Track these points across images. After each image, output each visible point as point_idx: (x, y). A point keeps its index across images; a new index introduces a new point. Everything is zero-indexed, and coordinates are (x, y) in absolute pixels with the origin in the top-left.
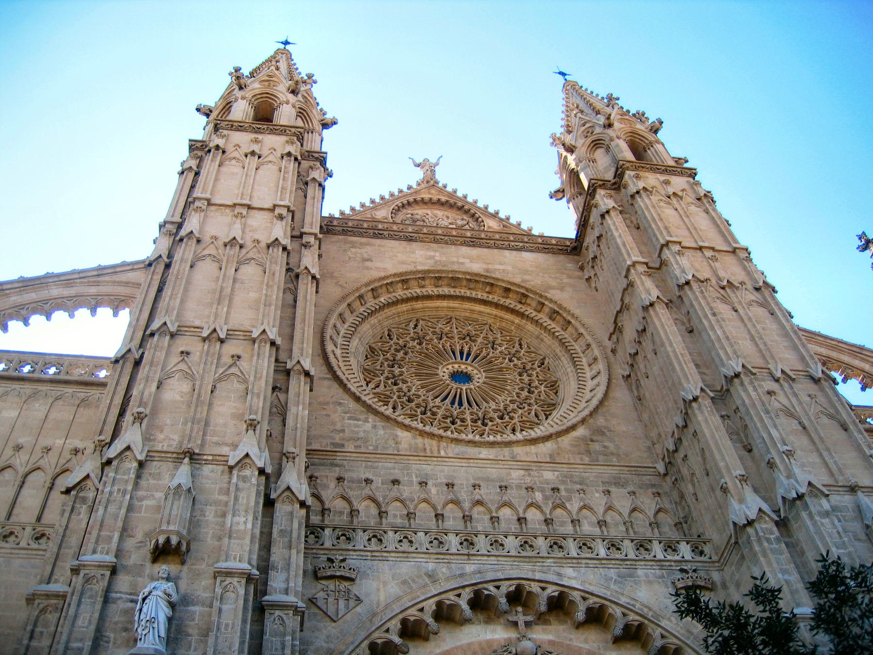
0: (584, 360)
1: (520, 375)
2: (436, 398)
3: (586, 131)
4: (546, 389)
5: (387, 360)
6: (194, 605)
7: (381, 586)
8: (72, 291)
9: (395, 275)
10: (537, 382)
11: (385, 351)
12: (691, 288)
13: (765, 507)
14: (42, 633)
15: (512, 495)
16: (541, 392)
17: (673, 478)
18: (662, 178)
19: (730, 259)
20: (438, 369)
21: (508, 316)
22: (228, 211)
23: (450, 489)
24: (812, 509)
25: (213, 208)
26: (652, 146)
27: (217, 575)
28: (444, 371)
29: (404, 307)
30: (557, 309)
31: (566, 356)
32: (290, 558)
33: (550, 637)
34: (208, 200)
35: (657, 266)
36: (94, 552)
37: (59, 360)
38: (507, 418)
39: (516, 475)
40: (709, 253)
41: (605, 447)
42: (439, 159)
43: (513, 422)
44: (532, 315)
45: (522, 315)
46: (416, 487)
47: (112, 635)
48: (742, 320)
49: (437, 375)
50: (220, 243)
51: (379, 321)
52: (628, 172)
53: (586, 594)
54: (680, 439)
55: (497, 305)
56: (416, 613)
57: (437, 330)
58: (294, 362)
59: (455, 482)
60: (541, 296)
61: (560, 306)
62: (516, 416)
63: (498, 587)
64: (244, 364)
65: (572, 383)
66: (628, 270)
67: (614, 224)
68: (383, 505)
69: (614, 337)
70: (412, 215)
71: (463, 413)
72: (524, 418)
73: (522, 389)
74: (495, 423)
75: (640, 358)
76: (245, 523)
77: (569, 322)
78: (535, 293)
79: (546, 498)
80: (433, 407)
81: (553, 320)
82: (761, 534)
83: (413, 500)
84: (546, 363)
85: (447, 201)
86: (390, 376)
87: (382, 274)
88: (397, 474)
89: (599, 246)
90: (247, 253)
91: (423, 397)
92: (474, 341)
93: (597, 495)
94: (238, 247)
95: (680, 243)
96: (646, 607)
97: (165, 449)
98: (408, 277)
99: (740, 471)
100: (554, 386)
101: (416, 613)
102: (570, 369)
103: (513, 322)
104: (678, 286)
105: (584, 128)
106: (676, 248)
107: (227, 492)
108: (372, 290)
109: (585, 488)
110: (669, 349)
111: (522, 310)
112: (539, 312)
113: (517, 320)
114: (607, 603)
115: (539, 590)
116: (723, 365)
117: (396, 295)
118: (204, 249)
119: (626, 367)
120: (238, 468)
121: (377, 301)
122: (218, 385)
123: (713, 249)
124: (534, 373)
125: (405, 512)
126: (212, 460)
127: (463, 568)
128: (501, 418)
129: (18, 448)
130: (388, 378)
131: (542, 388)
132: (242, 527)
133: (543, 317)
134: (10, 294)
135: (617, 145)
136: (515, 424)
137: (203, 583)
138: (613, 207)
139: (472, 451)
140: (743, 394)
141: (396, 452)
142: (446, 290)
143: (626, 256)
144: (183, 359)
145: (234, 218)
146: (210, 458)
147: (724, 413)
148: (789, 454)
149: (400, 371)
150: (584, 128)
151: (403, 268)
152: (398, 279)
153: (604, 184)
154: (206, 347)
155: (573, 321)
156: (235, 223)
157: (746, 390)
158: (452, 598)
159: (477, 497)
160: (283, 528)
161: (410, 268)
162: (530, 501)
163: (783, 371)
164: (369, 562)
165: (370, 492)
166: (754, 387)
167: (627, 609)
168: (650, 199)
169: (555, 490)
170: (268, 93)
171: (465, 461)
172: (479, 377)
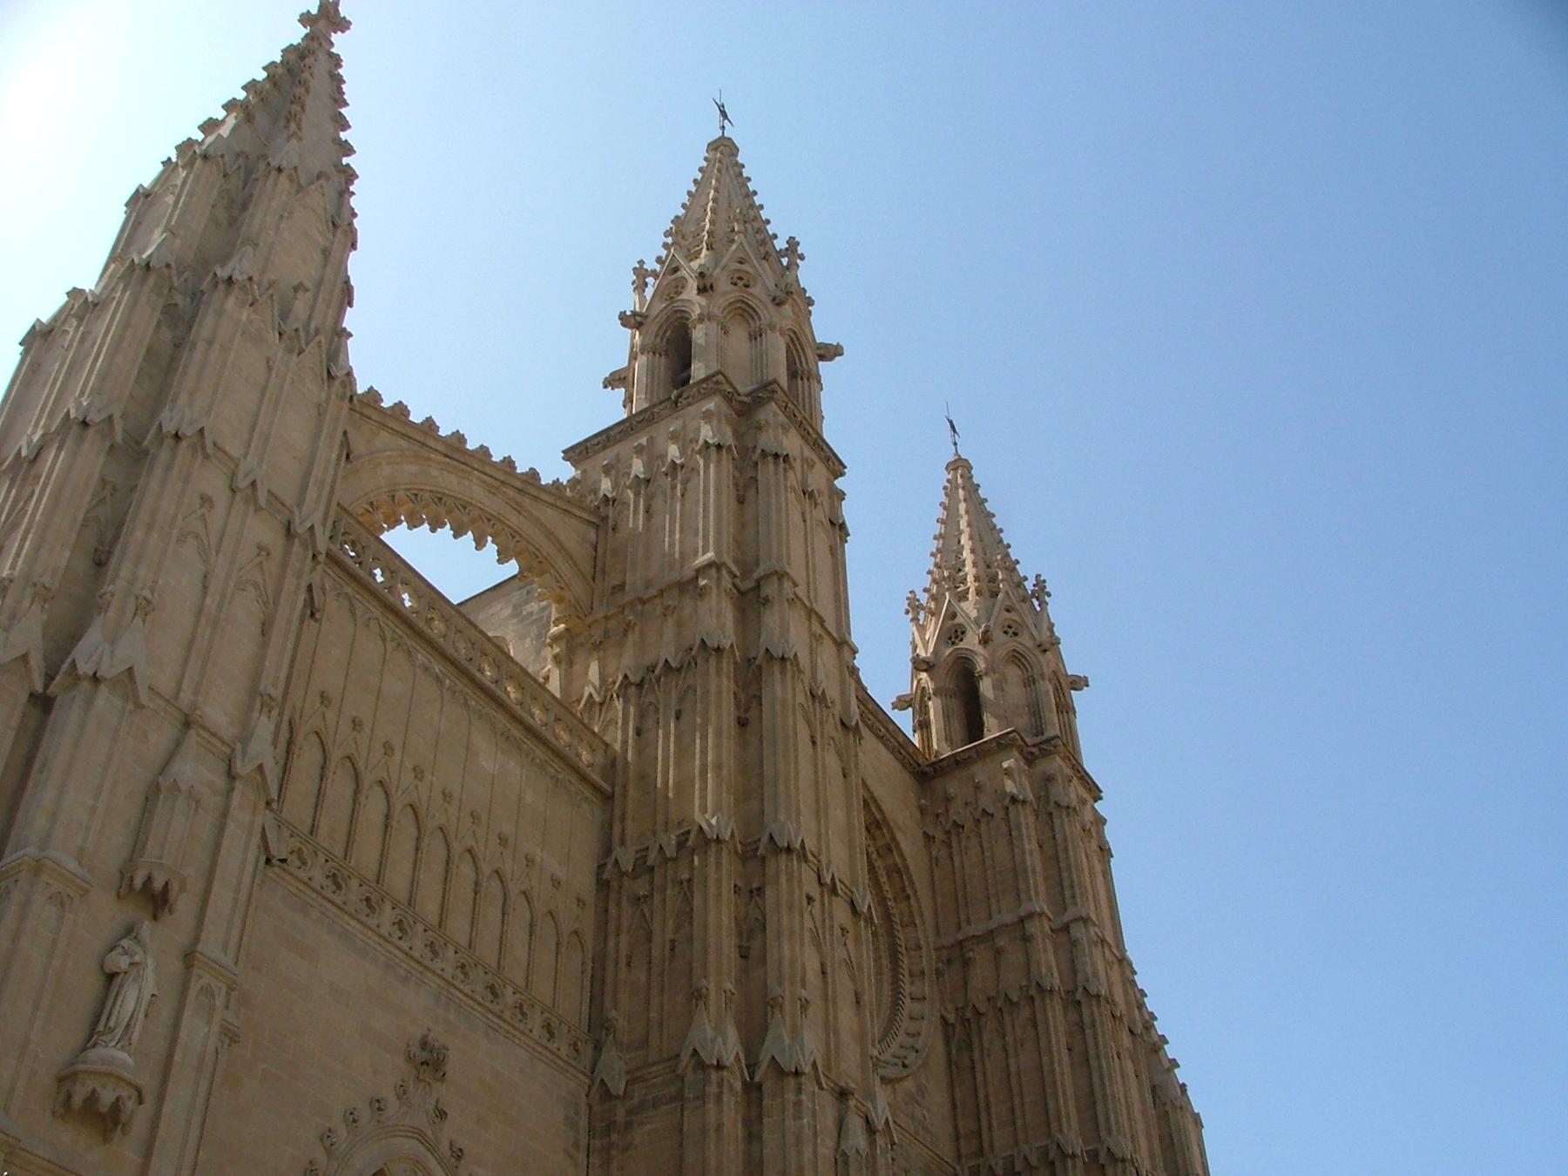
12: (1099, 1002)
30: (900, 866)
41: (924, 1117)
61: (907, 867)
69: (945, 953)
77: (908, 897)
119: (949, 1006)
123: (1110, 946)
135: (1047, 692)
155: (912, 901)
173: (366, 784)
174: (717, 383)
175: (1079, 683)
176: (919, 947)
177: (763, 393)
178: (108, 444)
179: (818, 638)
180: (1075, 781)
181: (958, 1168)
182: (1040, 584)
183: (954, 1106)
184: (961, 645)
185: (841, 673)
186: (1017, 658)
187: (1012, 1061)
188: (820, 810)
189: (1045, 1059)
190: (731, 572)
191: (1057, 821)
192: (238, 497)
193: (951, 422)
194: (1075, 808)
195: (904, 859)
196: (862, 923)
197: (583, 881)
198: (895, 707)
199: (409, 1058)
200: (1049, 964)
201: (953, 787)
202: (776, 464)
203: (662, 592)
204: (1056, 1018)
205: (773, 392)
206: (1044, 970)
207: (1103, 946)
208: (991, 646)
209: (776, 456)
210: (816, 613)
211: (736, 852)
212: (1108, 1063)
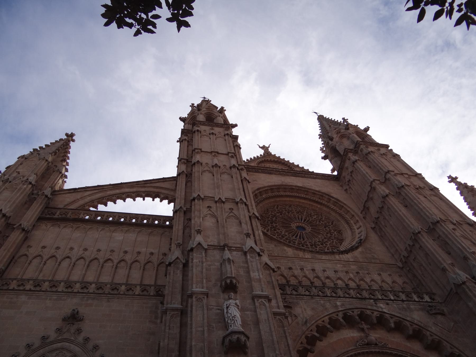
0: (352, 221)
1: (325, 227)
2: (293, 236)
3: (337, 132)
4: (337, 234)
5: (269, 220)
6: (247, 311)
7: (304, 310)
8: (134, 190)
9: (268, 186)
10: (333, 231)
11: (268, 217)
12: (405, 188)
13: (469, 277)
14: (173, 327)
15: (341, 275)
16: (335, 235)
17: (408, 269)
18: (376, 148)
20: (291, 225)
21: (315, 204)
22: (209, 154)
23: (314, 272)
25: (203, 153)
26: (367, 137)
27: (254, 297)
28: (294, 226)
29: (272, 200)
31: (343, 220)
32: (275, 293)
33: (379, 336)
34: (201, 149)
35: (383, 181)
36: (197, 288)
37: (136, 216)
38: (325, 245)
39: (339, 267)
40: (406, 176)
41: (373, 256)
42: (269, 145)
43: (328, 246)
44: (326, 204)
45: (321, 204)
46: (300, 271)
47: (214, 325)
48: (431, 202)
49: (291, 227)
50: (210, 166)
51: (263, 205)
52: (362, 146)
53: (392, 316)
54: (411, 251)
55: (310, 200)
56: (321, 323)
57: (286, 209)
58: (252, 213)
59: (316, 269)
60: (328, 195)
61: (338, 200)
62: (328, 244)
63: (353, 312)
64: (235, 212)
65: (348, 231)
66: (371, 183)
67: (360, 165)
68: (288, 278)
69: (364, 212)
70: (264, 165)
71: (306, 242)
72: (331, 245)
73: (327, 233)
74: (320, 246)
76: (259, 275)
77: (343, 206)
78: (326, 194)
79: (355, 276)
80: (293, 240)
81: (335, 206)
82: (470, 288)
83: (300, 276)
84: (334, 224)
85: (277, 161)
86: (272, 227)
87: (262, 186)
88: (290, 265)
89: (351, 176)
90: (222, 170)
91: (288, 236)
92: (303, 214)
93: (376, 275)
94: (218, 168)
95: (394, 171)
96: (419, 321)
97: (212, 244)
98: (273, 187)
99: (450, 262)
100: (340, 232)
101: (321, 323)
102: (346, 226)
103: (317, 207)
104: (398, 188)
105: (335, 131)
106: (392, 173)
107: (247, 262)
108: (260, 192)
109: (370, 272)
110: (401, 213)
111: (321, 202)
112: (329, 202)
113: (319, 206)
114: (401, 320)
115: (370, 313)
116: (429, 218)
117: (269, 195)
118: (204, 168)
120: (248, 253)
121: (262, 197)
122: (227, 220)
123: (407, 174)
124: (330, 227)
125: (297, 281)
126: (235, 250)
127: (336, 304)
128: (322, 244)
129: (126, 252)
130: (271, 228)
131: (335, 232)
132: (258, 277)
134: (107, 190)
135: (353, 136)
136: (328, 247)
137: (248, 301)
138: (358, 159)
139: (319, 256)
140: (443, 229)
141: (287, 256)
142: (288, 193)
143: (369, 178)
144: (209, 210)
145: (213, 157)
146: (234, 249)
147: (433, 238)
149: (275, 225)
150: (335, 131)
151: (270, 184)
152: (269, 188)
153: (351, 151)
154: (218, 205)
156: (214, 159)
157: (444, 228)
158: (335, 316)
159: (326, 275)
160: (268, 280)
161: (273, 184)
162: (349, 277)
163: (457, 221)
164: (295, 301)
165: (281, 273)
166: (447, 226)
167: (412, 323)
168: (375, 155)
169: (358, 273)
170: (210, 113)
171: (317, 260)
172: (309, 229)
175: (367, 129)
176: (353, 216)
181: (398, 264)
182: (343, 119)
183: (387, 248)
187: (391, 222)
191: (369, 159)
193: (315, 113)
195: (335, 199)
198: (332, 172)
200: (382, 190)
204: (394, 202)
206: (382, 193)
207: (403, 175)
208: (334, 140)
212: (417, 201)
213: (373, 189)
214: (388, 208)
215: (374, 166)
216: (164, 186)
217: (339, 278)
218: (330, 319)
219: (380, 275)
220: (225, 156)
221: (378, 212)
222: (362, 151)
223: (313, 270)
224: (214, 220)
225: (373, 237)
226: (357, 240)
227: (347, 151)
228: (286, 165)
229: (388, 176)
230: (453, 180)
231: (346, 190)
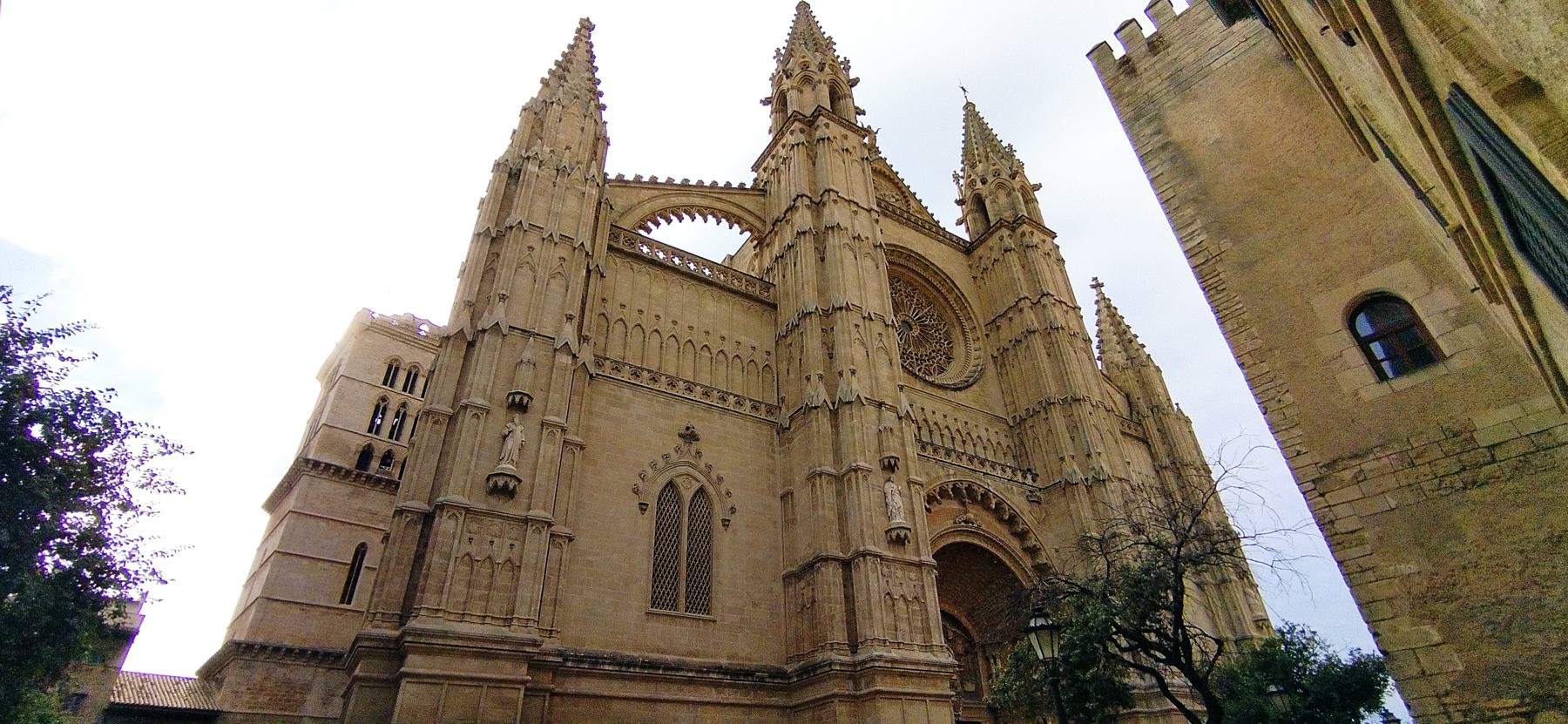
15: (950, 421)
19: (1071, 312)
21: (930, 288)
24: (1108, 487)
45: (939, 291)
53: (995, 496)
61: (963, 295)
66: (1020, 300)
75: (1011, 352)
77: (966, 307)
81: (956, 302)
89: (993, 264)
105: (994, 167)
116: (1071, 387)
119: (995, 349)
133: (951, 298)
135: (1018, 197)
148: (1099, 454)
150: (994, 167)
173: (648, 333)
174: (796, 116)
175: (1038, 187)
176: (975, 328)
177: (819, 111)
178: (490, 239)
179: (855, 212)
180: (1035, 231)
182: (1010, 146)
183: (1003, 393)
184: (977, 187)
185: (871, 222)
186: (1001, 186)
187: (1022, 366)
188: (862, 287)
189: (1036, 362)
190: (808, 197)
191: (1028, 254)
192: (545, 242)
193: (962, 88)
194: (1036, 246)
196: (890, 329)
197: (770, 344)
199: (681, 436)
200: (1031, 318)
201: (980, 251)
202: (824, 143)
203: (785, 214)
204: (1038, 342)
205: (820, 111)
206: (1029, 323)
209: (823, 139)
210: (854, 202)
211: (820, 315)
212: (1067, 359)
213: (1016, 307)
214: (1028, 347)
215: (1030, 271)
216: (746, 206)
217: (947, 427)
218: (940, 488)
219: (987, 430)
220: (865, 212)
221: (1010, 341)
222: (1023, 234)
223: (923, 409)
224: (863, 351)
225: (991, 371)
226: (971, 368)
227: (1001, 224)
228: (903, 193)
229: (1045, 300)
230: (1097, 285)
231: (975, 278)
